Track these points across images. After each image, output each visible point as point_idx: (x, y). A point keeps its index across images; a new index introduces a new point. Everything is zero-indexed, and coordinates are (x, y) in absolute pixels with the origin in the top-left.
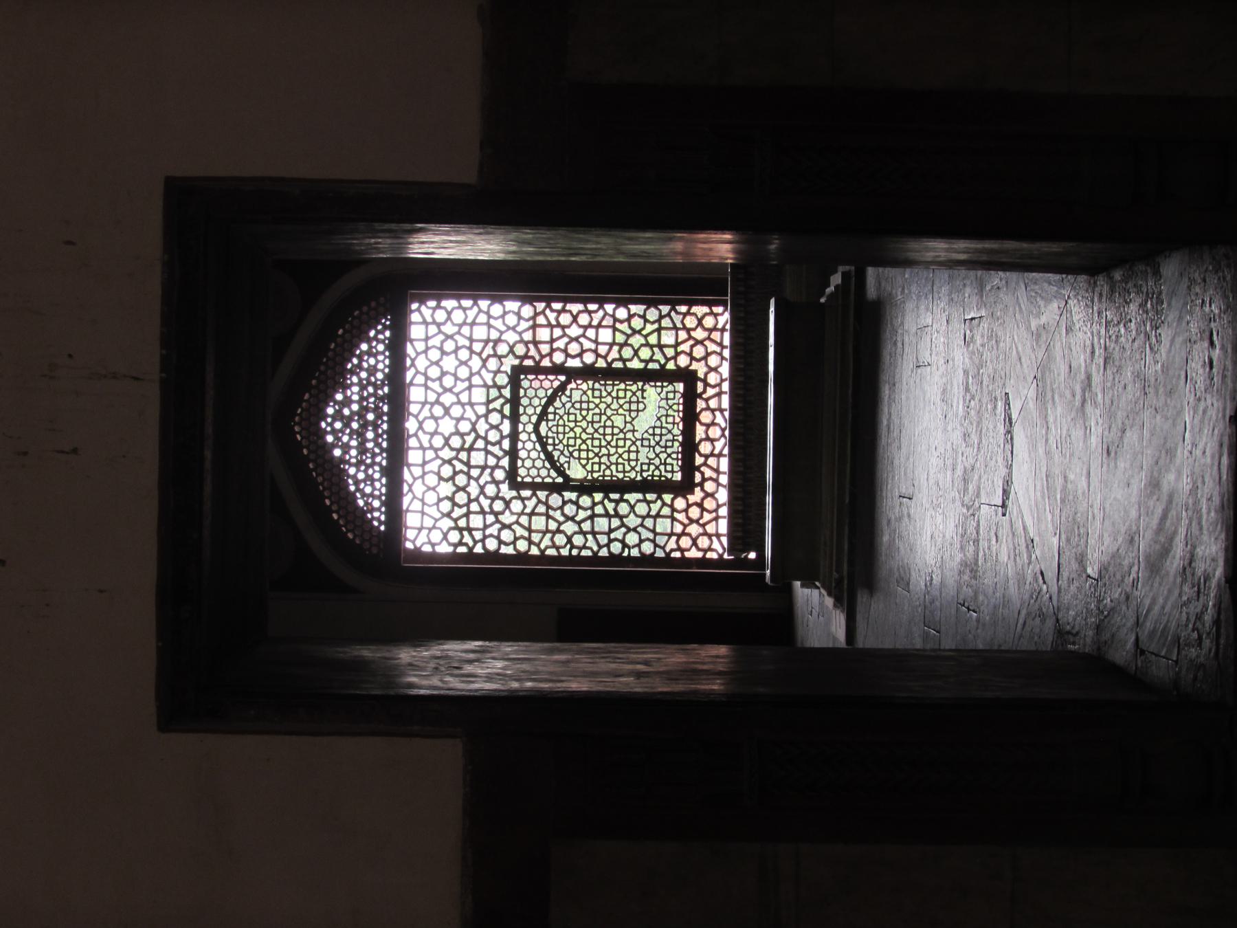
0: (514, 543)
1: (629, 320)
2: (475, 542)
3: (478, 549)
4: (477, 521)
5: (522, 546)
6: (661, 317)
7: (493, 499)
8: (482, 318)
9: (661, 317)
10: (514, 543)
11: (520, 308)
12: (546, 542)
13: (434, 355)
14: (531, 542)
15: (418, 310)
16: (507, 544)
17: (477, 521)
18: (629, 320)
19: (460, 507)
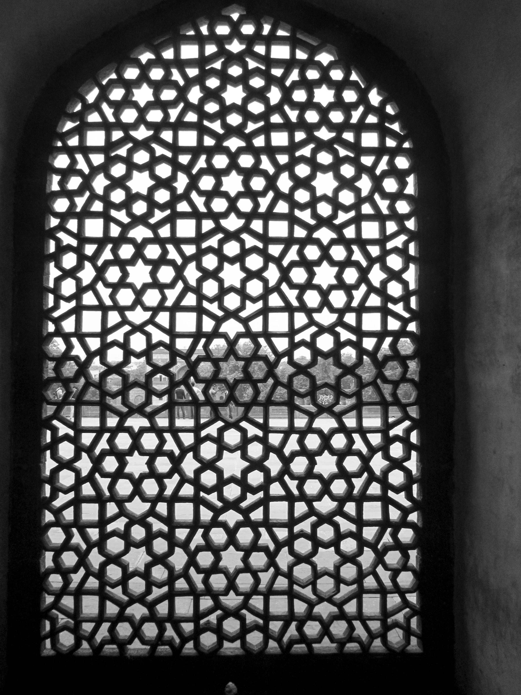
1: (398, 545)
2: (57, 321)
4: (91, 321)
6: (402, 593)
7: (125, 346)
8: (394, 325)
9: (402, 593)
11: (412, 381)
13: (338, 253)
15: (402, 230)
17: (91, 321)
18: (398, 545)
19: (112, 296)
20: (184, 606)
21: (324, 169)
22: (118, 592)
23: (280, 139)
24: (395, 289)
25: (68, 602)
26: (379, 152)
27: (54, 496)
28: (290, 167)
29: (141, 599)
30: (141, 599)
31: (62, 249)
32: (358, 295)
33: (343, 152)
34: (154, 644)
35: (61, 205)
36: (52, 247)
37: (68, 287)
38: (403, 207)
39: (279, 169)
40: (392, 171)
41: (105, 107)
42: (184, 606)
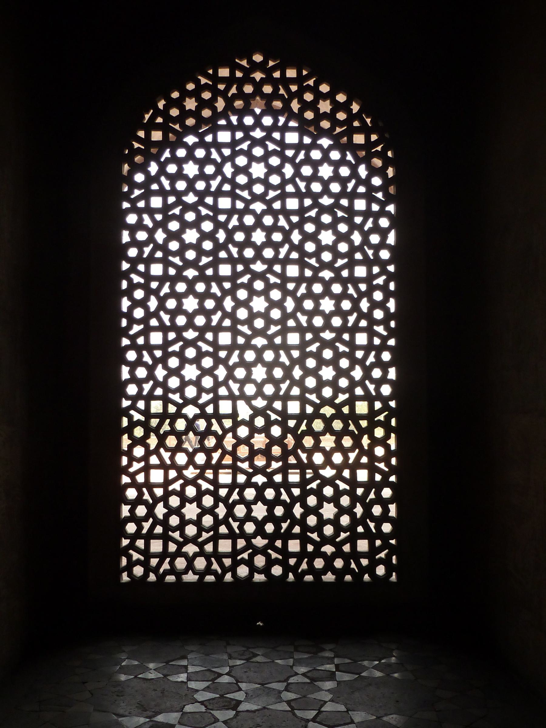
0: (134, 379)
1: (379, 500)
3: (125, 342)
5: (132, 390)
10: (134, 379)
11: (390, 382)
12: (137, 416)
14: (135, 399)
16: (132, 372)
17: (156, 338)
20: (225, 546)
21: (326, 227)
22: (176, 535)
23: (292, 204)
24: (378, 314)
25: (140, 543)
26: (367, 214)
27: (130, 465)
28: (300, 226)
29: (194, 540)
30: (194, 540)
31: (133, 287)
32: (352, 319)
33: (340, 214)
34: (202, 574)
35: (133, 252)
36: (124, 285)
37: (139, 313)
38: (385, 254)
39: (293, 226)
40: (376, 229)
41: (163, 179)
42: (225, 546)
